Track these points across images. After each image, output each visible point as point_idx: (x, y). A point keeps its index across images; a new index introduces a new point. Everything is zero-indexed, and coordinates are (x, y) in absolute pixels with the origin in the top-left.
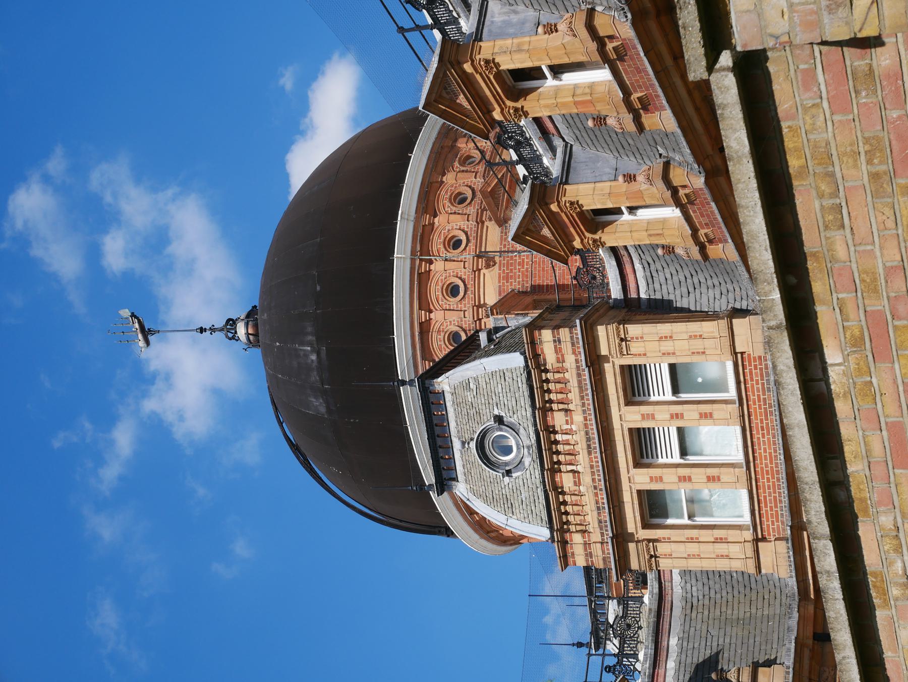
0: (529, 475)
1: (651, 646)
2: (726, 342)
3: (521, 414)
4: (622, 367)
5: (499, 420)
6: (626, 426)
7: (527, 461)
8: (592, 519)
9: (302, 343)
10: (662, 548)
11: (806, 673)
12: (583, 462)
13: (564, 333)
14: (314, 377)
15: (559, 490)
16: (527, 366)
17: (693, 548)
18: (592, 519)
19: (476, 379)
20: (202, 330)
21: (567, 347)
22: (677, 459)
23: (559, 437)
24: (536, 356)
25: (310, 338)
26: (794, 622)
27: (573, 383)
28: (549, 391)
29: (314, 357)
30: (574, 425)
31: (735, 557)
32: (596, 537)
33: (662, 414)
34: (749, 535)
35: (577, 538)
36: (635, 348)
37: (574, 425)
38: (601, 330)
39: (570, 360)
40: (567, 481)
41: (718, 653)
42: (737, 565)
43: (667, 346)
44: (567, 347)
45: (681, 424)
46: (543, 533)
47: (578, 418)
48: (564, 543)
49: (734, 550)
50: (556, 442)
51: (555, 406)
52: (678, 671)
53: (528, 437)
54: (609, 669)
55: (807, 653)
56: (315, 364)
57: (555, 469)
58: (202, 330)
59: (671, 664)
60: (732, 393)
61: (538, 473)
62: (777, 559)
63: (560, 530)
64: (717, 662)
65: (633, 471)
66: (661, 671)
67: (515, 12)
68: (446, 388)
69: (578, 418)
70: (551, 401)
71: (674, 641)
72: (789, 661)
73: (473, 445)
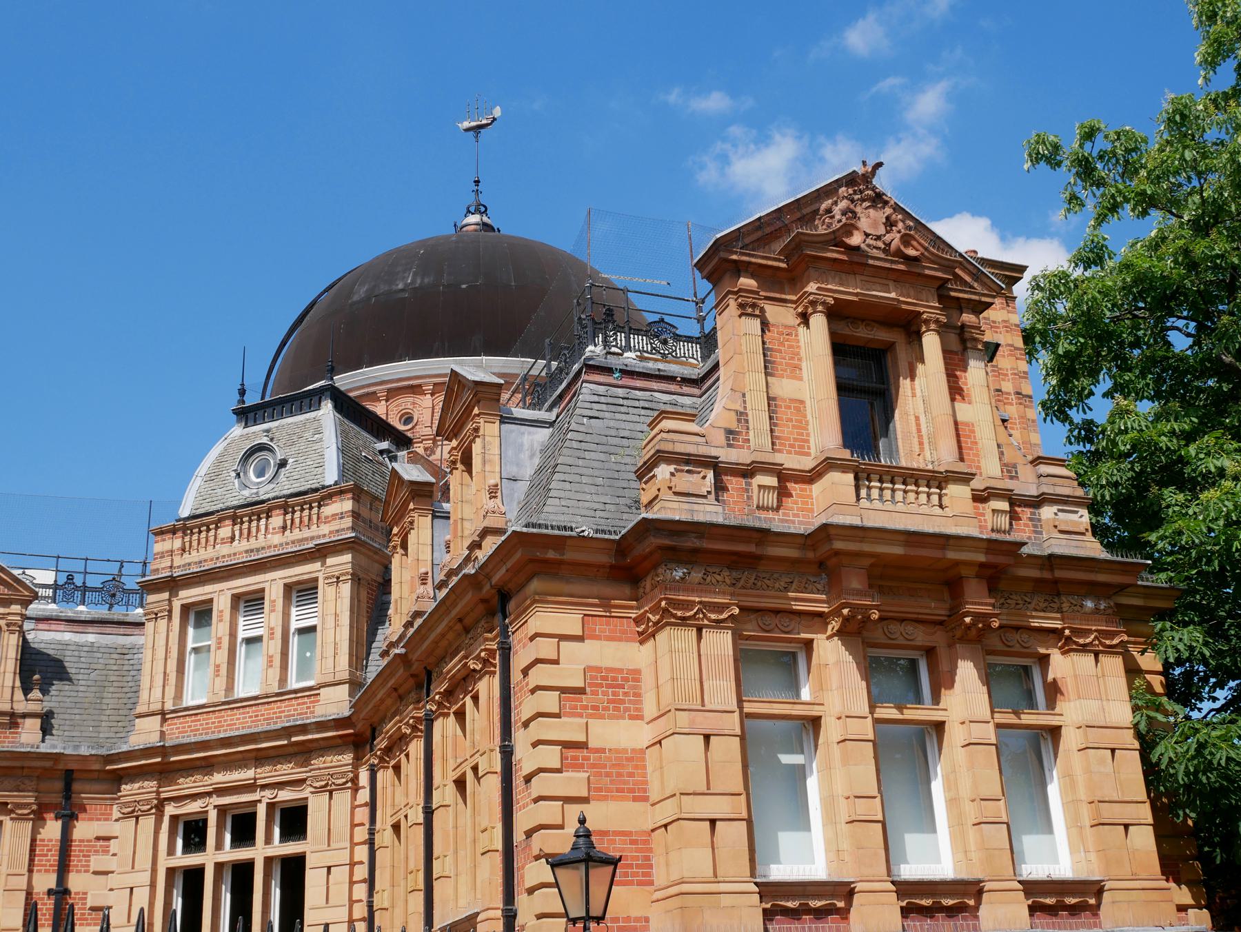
0: (236, 494)
1: (88, 617)
2: (330, 679)
3: (287, 484)
4: (316, 579)
5: (283, 464)
6: (266, 585)
7: (246, 493)
8: (194, 556)
9: (415, 274)
10: (162, 623)
11: (27, 764)
12: (241, 546)
13: (348, 522)
14: (383, 288)
15: (218, 524)
16: (324, 487)
17: (161, 653)
18: (194, 556)
19: (321, 440)
20: (477, 182)
21: (335, 525)
23: (263, 522)
24: (330, 496)
25: (419, 281)
26: (84, 751)
27: (306, 533)
28: (302, 510)
29: (400, 286)
30: (271, 536)
31: (152, 694)
32: (178, 561)
33: (276, 620)
34: (169, 706)
35: (178, 543)
36: (331, 591)
37: (271, 536)
38: (347, 557)
39: (325, 529)
40: (225, 531)
41: (70, 680)
42: (144, 695)
44: (335, 525)
45: (265, 639)
46: (185, 512)
47: (276, 539)
48: (174, 531)
49: (157, 693)
50: (259, 519)
51: (289, 516)
52: (59, 643)
53: (267, 491)
54: (70, 578)
55: (48, 764)
56: (394, 288)
57: (235, 519)
58: (477, 182)
59: (68, 636)
60: (293, 684)
61: (236, 503)
62: (146, 733)
63: (184, 527)
64: (61, 679)
65: (229, 594)
66: (62, 627)
67: (532, 456)
68: (321, 412)
69: (276, 539)
70: (294, 512)
71: (91, 638)
72: (44, 749)
73: (265, 440)
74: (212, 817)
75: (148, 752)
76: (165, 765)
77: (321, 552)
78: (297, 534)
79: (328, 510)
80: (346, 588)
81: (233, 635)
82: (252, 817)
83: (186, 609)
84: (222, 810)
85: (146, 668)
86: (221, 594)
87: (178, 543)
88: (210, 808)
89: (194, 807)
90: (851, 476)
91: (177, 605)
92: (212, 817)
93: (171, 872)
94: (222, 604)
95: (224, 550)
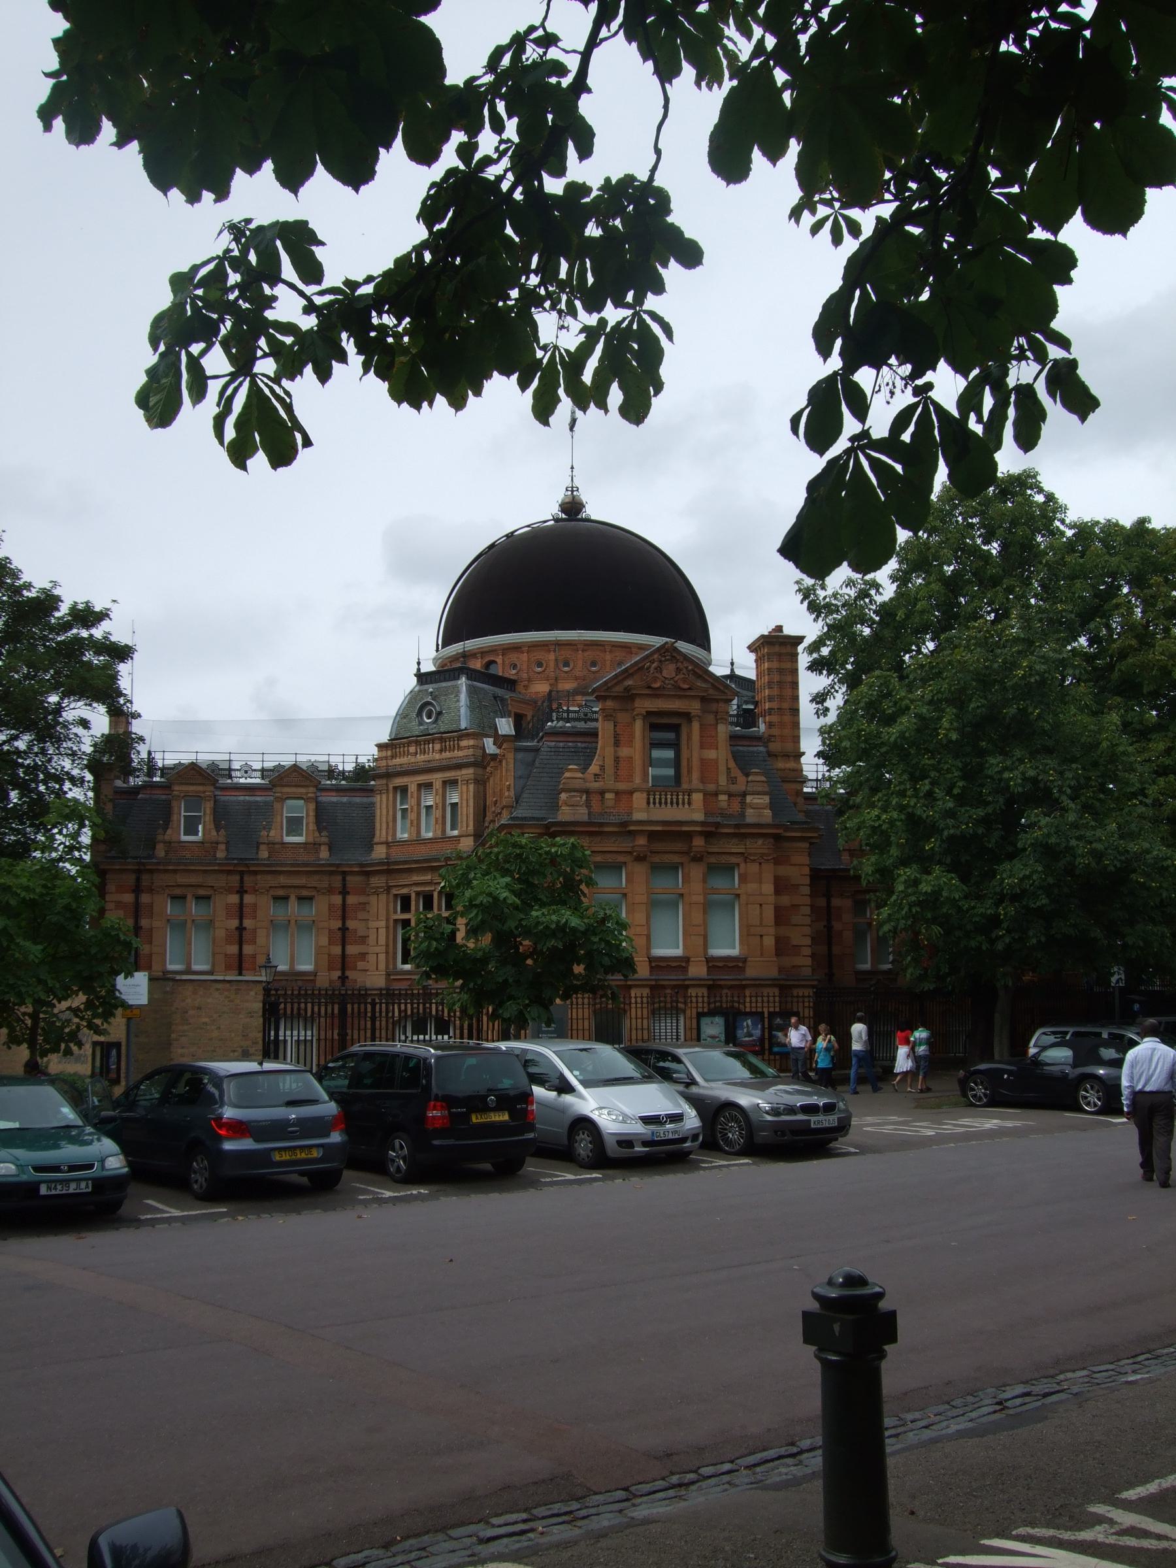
0: (417, 730)
5: (439, 714)
8: (398, 761)
12: (421, 758)
15: (409, 744)
18: (398, 761)
22: (423, 804)
30: (434, 754)
34: (390, 839)
35: (389, 753)
37: (434, 754)
39: (461, 754)
40: (412, 749)
42: (378, 833)
43: (465, 804)
47: (437, 756)
57: (417, 743)
62: (380, 852)
69: (437, 756)
74: (413, 896)
75: (381, 863)
76: (390, 869)
77: (459, 767)
78: (447, 754)
79: (464, 743)
80: (471, 787)
81: (419, 804)
82: (432, 896)
83: (395, 788)
84: (418, 894)
85: (378, 818)
86: (412, 782)
87: (389, 753)
88: (412, 891)
89: (405, 891)
90: (645, 795)
91: (391, 786)
92: (413, 896)
93: (396, 921)
94: (413, 788)
95: (413, 759)
